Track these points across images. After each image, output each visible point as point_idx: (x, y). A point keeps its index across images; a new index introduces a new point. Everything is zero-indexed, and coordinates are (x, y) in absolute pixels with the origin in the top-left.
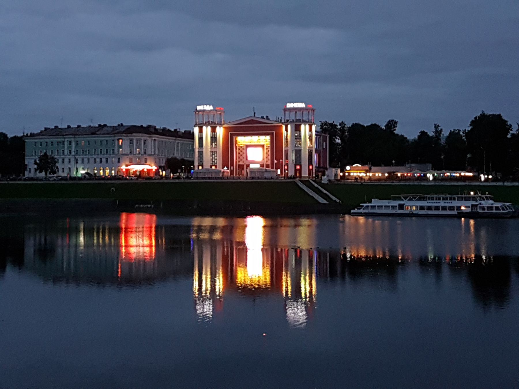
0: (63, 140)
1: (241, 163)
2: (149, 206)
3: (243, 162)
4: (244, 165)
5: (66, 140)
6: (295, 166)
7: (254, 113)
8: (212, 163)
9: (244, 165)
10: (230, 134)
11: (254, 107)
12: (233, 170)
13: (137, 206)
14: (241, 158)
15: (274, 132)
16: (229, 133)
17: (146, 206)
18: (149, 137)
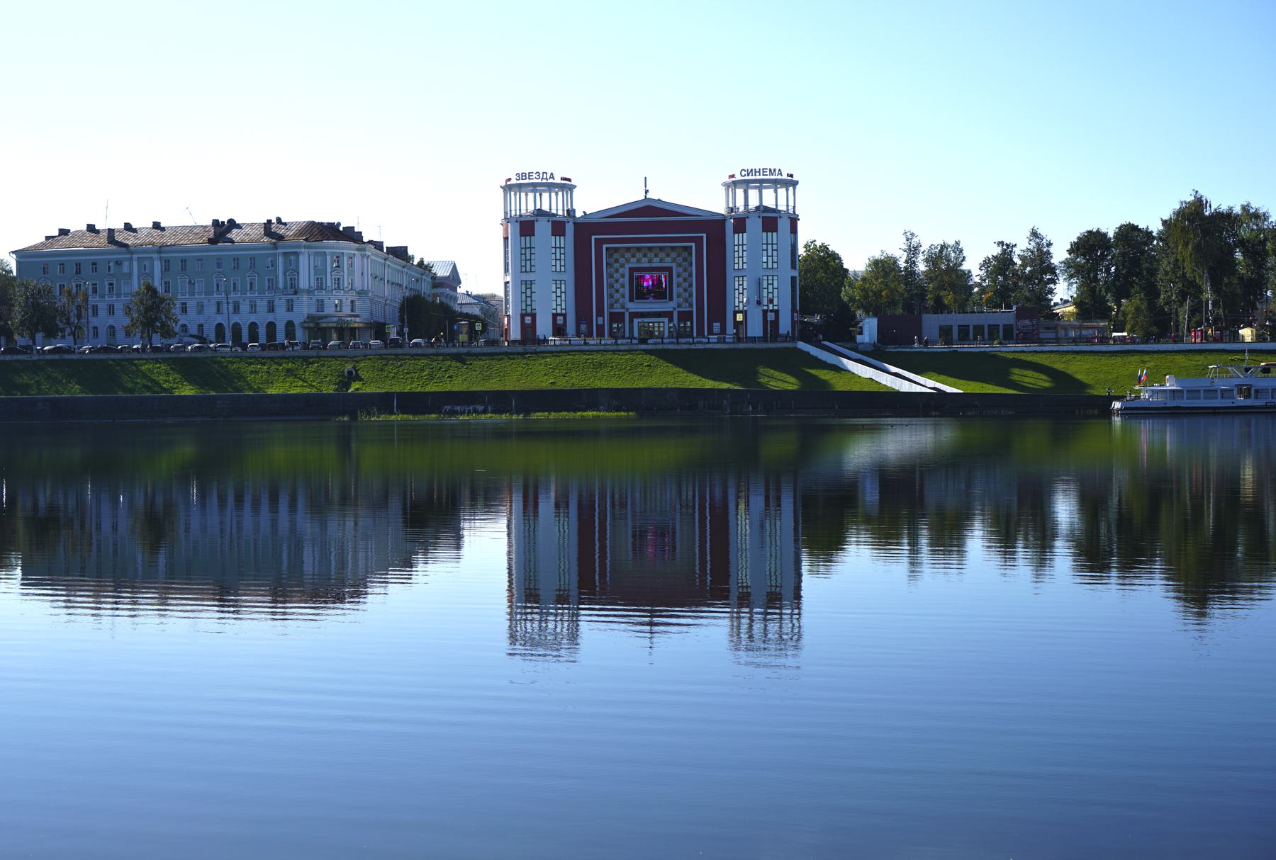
0: (129, 256)
1: (617, 309)
2: (480, 408)
3: (623, 307)
4: (623, 313)
5: (135, 256)
6: (765, 313)
7: (647, 192)
8: (556, 309)
9: (623, 313)
10: (595, 239)
11: (646, 178)
12: (604, 324)
13: (448, 408)
14: (617, 296)
15: (705, 235)
16: (593, 237)
17: (471, 408)
18: (358, 250)
